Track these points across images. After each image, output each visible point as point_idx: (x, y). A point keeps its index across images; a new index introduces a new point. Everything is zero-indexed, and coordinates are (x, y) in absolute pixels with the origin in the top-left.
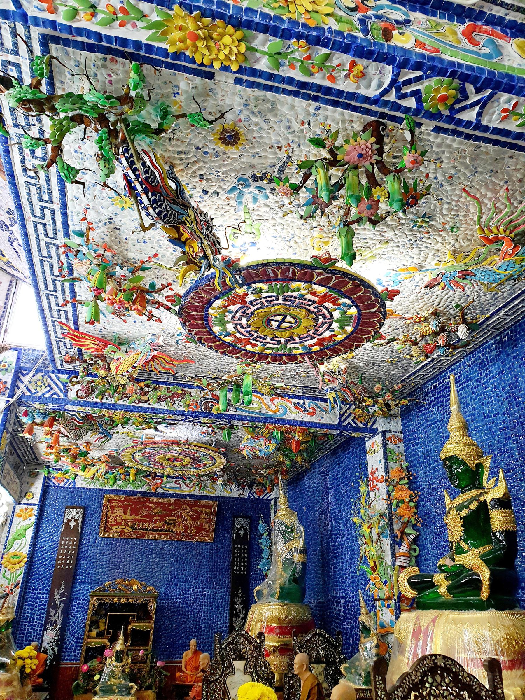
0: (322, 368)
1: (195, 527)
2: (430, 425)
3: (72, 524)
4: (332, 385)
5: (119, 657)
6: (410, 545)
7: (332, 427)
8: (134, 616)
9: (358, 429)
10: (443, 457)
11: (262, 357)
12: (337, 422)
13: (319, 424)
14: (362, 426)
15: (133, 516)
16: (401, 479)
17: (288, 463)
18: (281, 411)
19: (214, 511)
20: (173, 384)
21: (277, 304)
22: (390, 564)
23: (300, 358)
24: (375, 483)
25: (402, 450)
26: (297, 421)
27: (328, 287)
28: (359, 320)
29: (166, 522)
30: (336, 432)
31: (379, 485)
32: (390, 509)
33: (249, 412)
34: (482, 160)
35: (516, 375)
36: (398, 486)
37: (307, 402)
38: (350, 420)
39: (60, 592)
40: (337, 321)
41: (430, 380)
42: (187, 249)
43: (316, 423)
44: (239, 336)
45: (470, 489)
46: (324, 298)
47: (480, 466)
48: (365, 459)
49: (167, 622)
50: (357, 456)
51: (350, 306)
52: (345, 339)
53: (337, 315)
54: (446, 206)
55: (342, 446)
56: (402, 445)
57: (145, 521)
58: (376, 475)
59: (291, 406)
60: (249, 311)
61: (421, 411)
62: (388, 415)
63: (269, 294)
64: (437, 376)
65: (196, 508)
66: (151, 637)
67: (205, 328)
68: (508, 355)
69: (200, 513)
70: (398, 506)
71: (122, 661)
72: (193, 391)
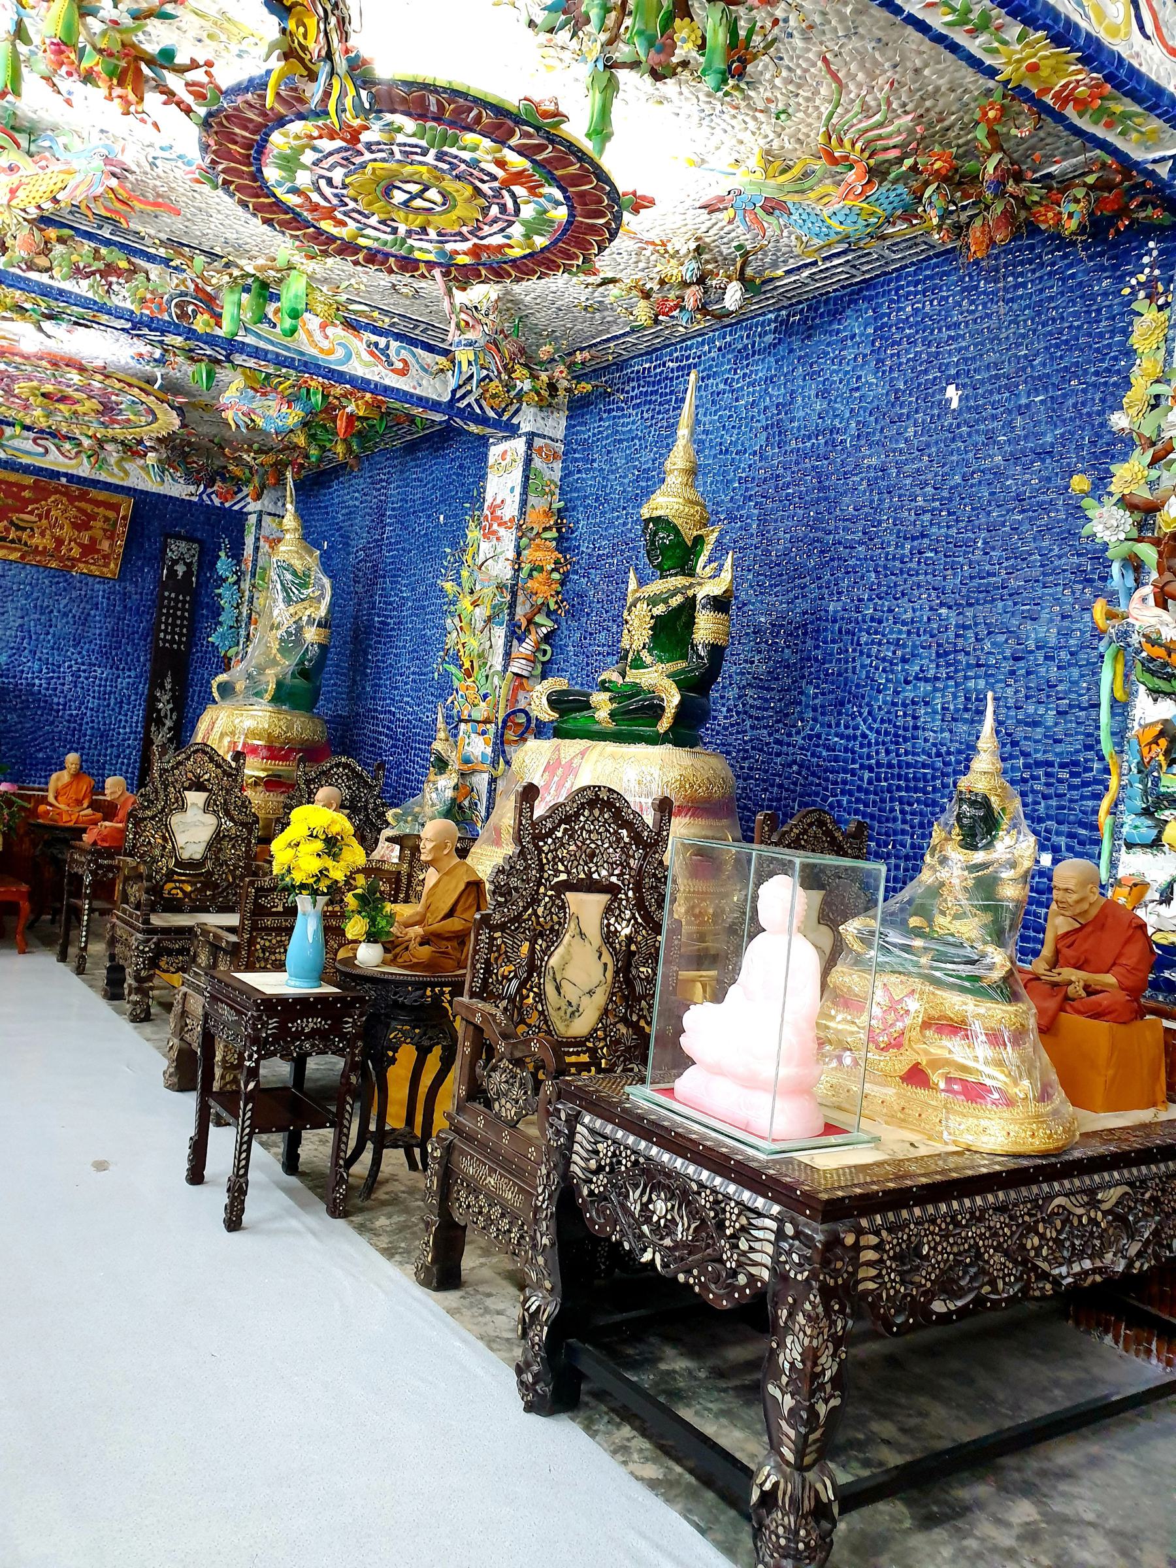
0: (460, 297)
2: (620, 441)
4: (470, 335)
6: (538, 643)
7: (435, 406)
9: (483, 421)
10: (647, 516)
11: (348, 249)
12: (446, 398)
13: (412, 395)
14: (492, 414)
16: (545, 529)
17: (314, 452)
18: (340, 353)
20: (108, 243)
21: (421, 163)
22: (499, 668)
23: (423, 269)
24: (495, 527)
25: (557, 475)
26: (368, 382)
27: (533, 161)
28: (565, 231)
29: (12, 523)
30: (439, 417)
31: (502, 531)
32: (516, 577)
33: (272, 343)
34: (872, 16)
35: (793, 392)
36: (538, 541)
37: (394, 345)
38: (471, 399)
40: (524, 223)
41: (641, 355)
42: (291, 25)
43: (405, 393)
44: (315, 197)
45: (676, 575)
46: (518, 177)
47: (699, 540)
48: (483, 477)
50: (461, 467)
51: (558, 203)
52: (524, 257)
53: (528, 211)
54: (785, 73)
55: (443, 442)
56: (558, 465)
58: (498, 513)
59: (362, 347)
60: (358, 160)
61: (610, 411)
62: (546, 405)
63: (414, 141)
64: (656, 350)
65: (83, 505)
67: (250, 165)
68: (791, 351)
69: (93, 517)
70: (530, 576)
72: (154, 270)
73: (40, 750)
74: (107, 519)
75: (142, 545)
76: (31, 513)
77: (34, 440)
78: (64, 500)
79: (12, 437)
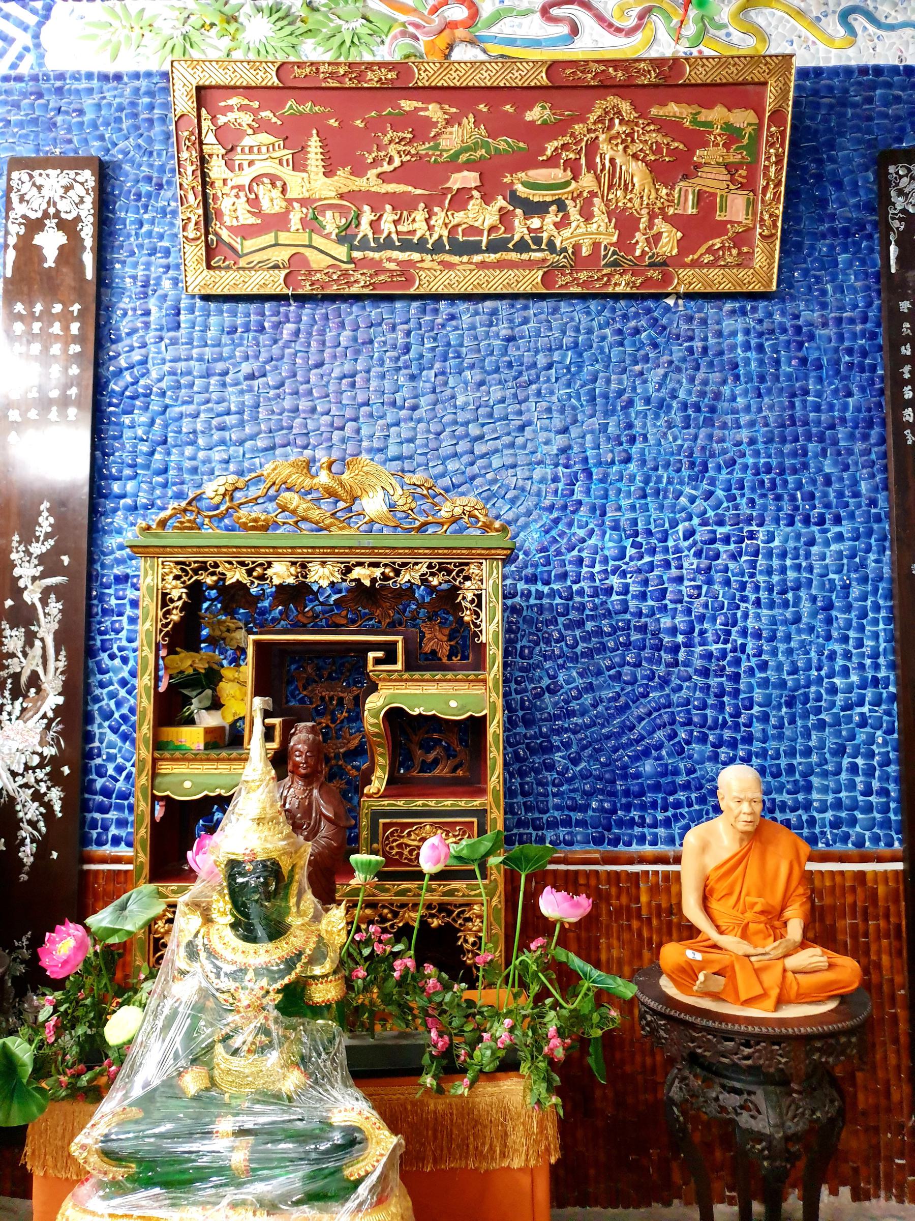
1: (676, 221)
3: (50, 242)
5: (257, 902)
15: (344, 180)
19: (777, 116)
29: (515, 199)
39: (37, 549)
49: (570, 677)
65: (673, 109)
69: (696, 138)
71: (277, 931)
73: (646, 753)
74: (732, 135)
75: (823, 202)
76: (552, 162)
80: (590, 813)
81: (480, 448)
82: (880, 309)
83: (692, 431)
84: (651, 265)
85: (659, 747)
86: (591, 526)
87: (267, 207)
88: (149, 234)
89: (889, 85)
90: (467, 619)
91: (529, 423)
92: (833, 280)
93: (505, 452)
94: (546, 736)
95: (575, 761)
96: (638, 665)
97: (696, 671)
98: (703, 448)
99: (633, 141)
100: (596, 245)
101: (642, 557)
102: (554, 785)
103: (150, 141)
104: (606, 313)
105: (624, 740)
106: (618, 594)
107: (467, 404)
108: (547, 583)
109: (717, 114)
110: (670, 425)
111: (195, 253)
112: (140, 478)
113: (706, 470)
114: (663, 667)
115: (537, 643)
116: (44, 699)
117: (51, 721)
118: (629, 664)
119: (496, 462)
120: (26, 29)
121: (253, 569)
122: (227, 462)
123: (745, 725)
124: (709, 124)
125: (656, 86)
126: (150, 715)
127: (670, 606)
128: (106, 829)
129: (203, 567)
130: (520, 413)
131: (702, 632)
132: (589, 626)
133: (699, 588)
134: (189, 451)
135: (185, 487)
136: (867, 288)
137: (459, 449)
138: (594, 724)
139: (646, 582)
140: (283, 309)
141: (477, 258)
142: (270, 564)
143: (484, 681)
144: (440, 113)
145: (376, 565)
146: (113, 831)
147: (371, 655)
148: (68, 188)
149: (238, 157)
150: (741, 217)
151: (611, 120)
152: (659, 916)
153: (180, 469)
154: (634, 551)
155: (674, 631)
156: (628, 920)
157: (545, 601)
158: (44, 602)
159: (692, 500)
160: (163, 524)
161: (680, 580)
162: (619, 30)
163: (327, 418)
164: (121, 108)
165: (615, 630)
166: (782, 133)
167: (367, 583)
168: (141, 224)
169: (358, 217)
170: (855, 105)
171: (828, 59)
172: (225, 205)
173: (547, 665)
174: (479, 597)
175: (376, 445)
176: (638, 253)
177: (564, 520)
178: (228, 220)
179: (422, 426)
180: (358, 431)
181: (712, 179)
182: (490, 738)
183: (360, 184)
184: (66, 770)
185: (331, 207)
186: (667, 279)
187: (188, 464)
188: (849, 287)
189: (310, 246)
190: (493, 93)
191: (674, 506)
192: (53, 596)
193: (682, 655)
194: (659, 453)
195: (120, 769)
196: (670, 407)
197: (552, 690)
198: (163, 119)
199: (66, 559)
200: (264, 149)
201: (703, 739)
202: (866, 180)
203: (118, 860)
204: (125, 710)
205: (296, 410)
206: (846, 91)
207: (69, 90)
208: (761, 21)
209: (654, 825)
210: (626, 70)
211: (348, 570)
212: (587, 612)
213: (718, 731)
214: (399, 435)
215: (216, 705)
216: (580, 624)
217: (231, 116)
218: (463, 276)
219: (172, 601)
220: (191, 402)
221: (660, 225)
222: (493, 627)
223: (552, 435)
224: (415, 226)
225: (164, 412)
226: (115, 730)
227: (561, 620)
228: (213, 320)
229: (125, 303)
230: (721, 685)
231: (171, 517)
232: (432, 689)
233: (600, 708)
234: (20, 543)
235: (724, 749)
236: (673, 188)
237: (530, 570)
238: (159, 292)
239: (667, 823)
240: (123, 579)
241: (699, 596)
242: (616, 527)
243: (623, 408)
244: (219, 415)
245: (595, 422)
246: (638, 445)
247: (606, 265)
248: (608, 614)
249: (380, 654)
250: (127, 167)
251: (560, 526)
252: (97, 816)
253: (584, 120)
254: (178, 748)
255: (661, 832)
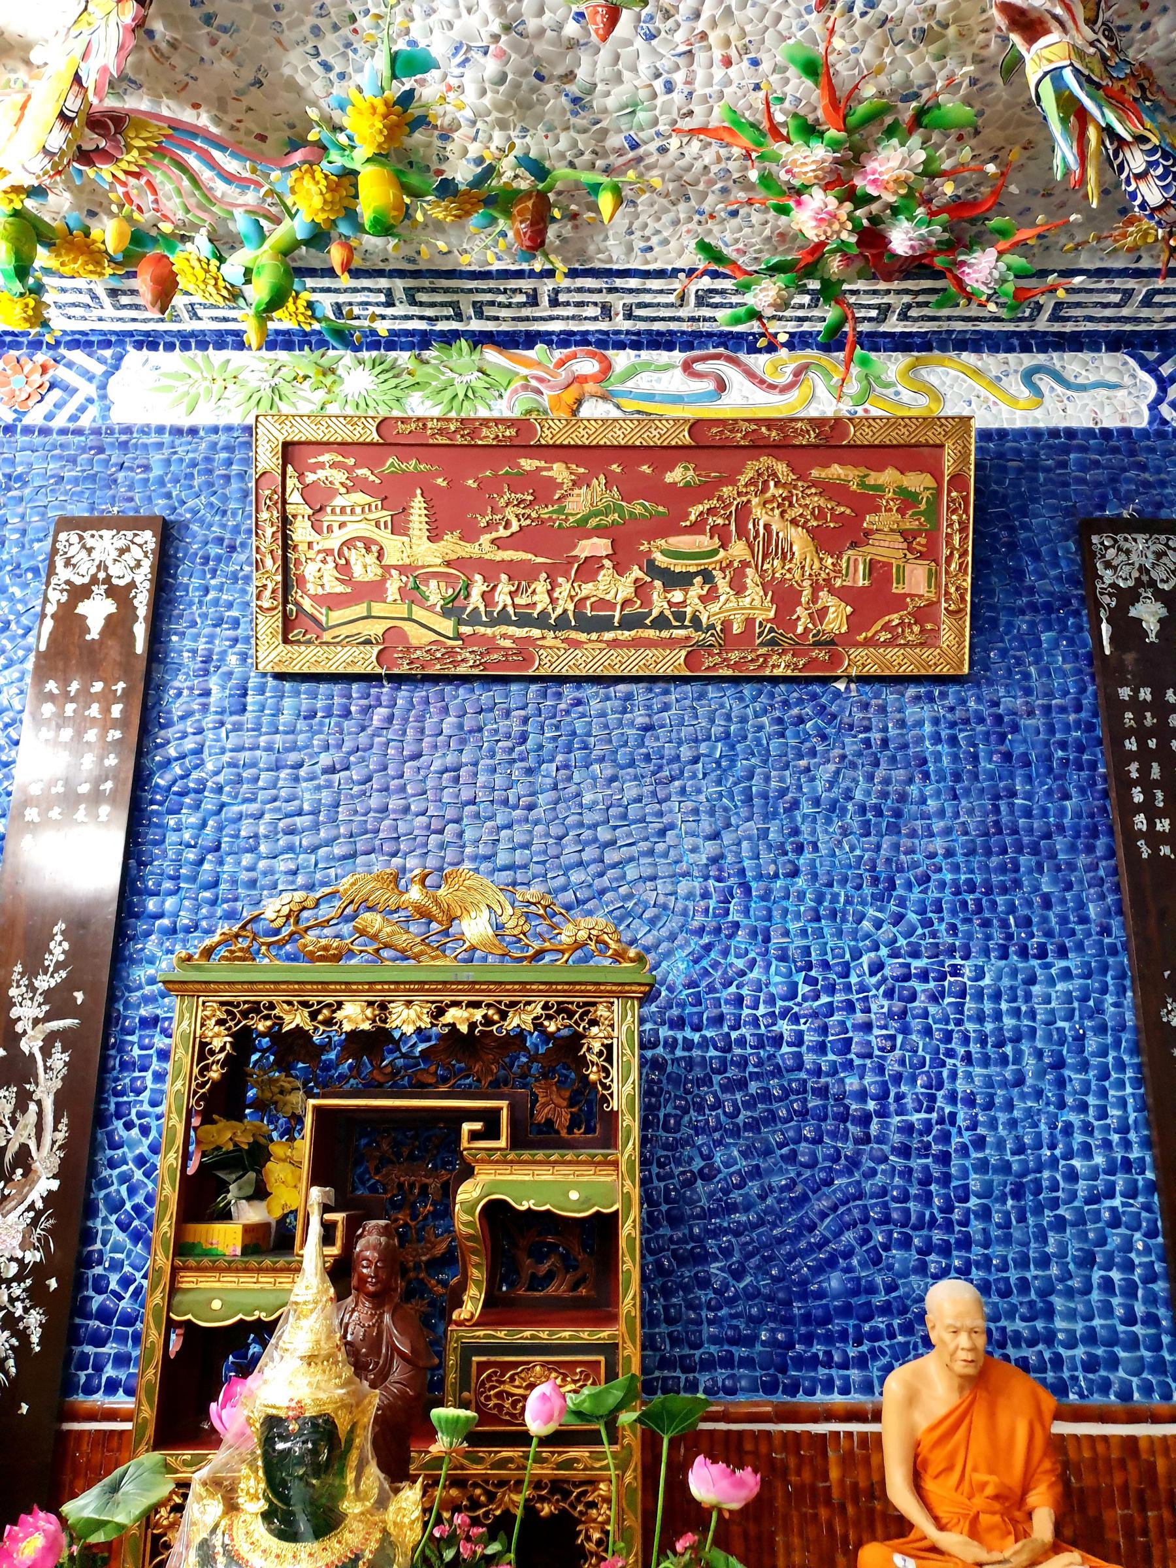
3: (96, 611)
8: (490, 1119)
15: (451, 546)
19: (957, 480)
29: (653, 569)
39: (43, 983)
49: (730, 1157)
57: (521, 575)
65: (836, 471)
66: (630, 1266)
69: (867, 502)
73: (831, 1262)
74: (907, 500)
75: (1019, 574)
76: (696, 528)
77: (687, 367)
78: (781, 468)
79: (632, 372)
80: (759, 1347)
81: (611, 856)
82: (1095, 695)
83: (873, 839)
84: (816, 644)
85: (848, 1254)
86: (752, 955)
87: (358, 573)
88: (216, 602)
89: (1084, 449)
90: (593, 1077)
91: (672, 827)
92: (1037, 662)
93: (643, 861)
94: (699, 1240)
95: (738, 1275)
96: (818, 1141)
97: (893, 1149)
98: (888, 861)
99: (791, 505)
100: (750, 622)
101: (817, 997)
102: (710, 1309)
103: (225, 499)
104: (763, 699)
105: (803, 1245)
106: (789, 1044)
107: (595, 803)
108: (697, 1028)
109: (888, 477)
110: (845, 832)
111: (269, 625)
112: (182, 893)
113: (893, 887)
114: (850, 1145)
115: (686, 1111)
116: (34, 1183)
117: (39, 1214)
118: (806, 1139)
119: (631, 872)
120: (90, 379)
121: (319, 1011)
122: (294, 873)
123: (960, 1224)
124: (879, 488)
125: (816, 446)
126: (173, 1207)
127: (857, 1062)
128: (99, 1369)
129: (255, 1008)
130: (660, 814)
131: (899, 1097)
132: (753, 1087)
133: (892, 1038)
134: (246, 860)
135: (239, 904)
136: (1079, 672)
137: (585, 856)
138: (761, 1222)
139: (824, 1030)
140: (373, 691)
141: (608, 636)
142: (340, 1005)
143: (615, 1164)
144: (566, 473)
145: (476, 1005)
146: (110, 1372)
147: (466, 1127)
148: (122, 551)
149: (327, 518)
150: (922, 589)
151: (765, 482)
152: (856, 1501)
153: (234, 882)
154: (807, 988)
155: (862, 1095)
156: (814, 1506)
157: (696, 1053)
158: (46, 1052)
159: (878, 925)
160: (208, 953)
161: (867, 1027)
162: (772, 387)
163: (422, 820)
164: (193, 464)
165: (787, 1092)
166: (966, 499)
167: (464, 1029)
168: (207, 591)
169: (467, 587)
170: (1048, 470)
171: (1014, 420)
172: (310, 571)
173: (700, 1140)
174: (609, 1047)
175: (482, 851)
176: (800, 630)
177: (718, 947)
178: (312, 588)
179: (539, 829)
180: (460, 835)
181: (887, 548)
182: (622, 1243)
183: (470, 550)
184: (53, 1284)
185: (435, 575)
186: (835, 660)
187: (244, 876)
188: (1057, 670)
189: (410, 619)
190: (627, 452)
191: (855, 931)
192: (58, 1045)
193: (874, 1128)
194: (833, 865)
195: (126, 1282)
196: (844, 810)
197: (706, 1176)
198: (242, 476)
199: (79, 996)
200: (358, 510)
201: (906, 1243)
202: (1067, 550)
203: (111, 1415)
204: (139, 1199)
205: (384, 809)
206: (1037, 455)
207: (136, 446)
208: (933, 380)
209: (844, 1365)
210: (781, 429)
211: (441, 1012)
212: (751, 1069)
213: (925, 1232)
214: (511, 839)
215: (260, 1193)
216: (742, 1084)
217: (321, 474)
218: (590, 655)
219: (212, 1053)
220: (254, 800)
221: (825, 598)
222: (628, 1089)
223: (700, 841)
224: (536, 598)
225: (219, 812)
226: (123, 1226)
227: (716, 1079)
228: (287, 702)
229: (180, 682)
230: (926, 1168)
231: (219, 944)
232: (545, 1175)
233: (769, 1201)
234: (22, 974)
235: (933, 1257)
236: (839, 557)
237: (675, 1012)
238: (223, 669)
239: (862, 1362)
240: (151, 1023)
241: (893, 1048)
242: (783, 958)
243: (786, 810)
244: (287, 816)
245: (752, 827)
246: (807, 855)
247: (762, 644)
248: (778, 1072)
249: (478, 1126)
250: (195, 527)
251: (713, 955)
252: (89, 1349)
253: (734, 483)
254: (206, 1253)
255: (854, 1374)
